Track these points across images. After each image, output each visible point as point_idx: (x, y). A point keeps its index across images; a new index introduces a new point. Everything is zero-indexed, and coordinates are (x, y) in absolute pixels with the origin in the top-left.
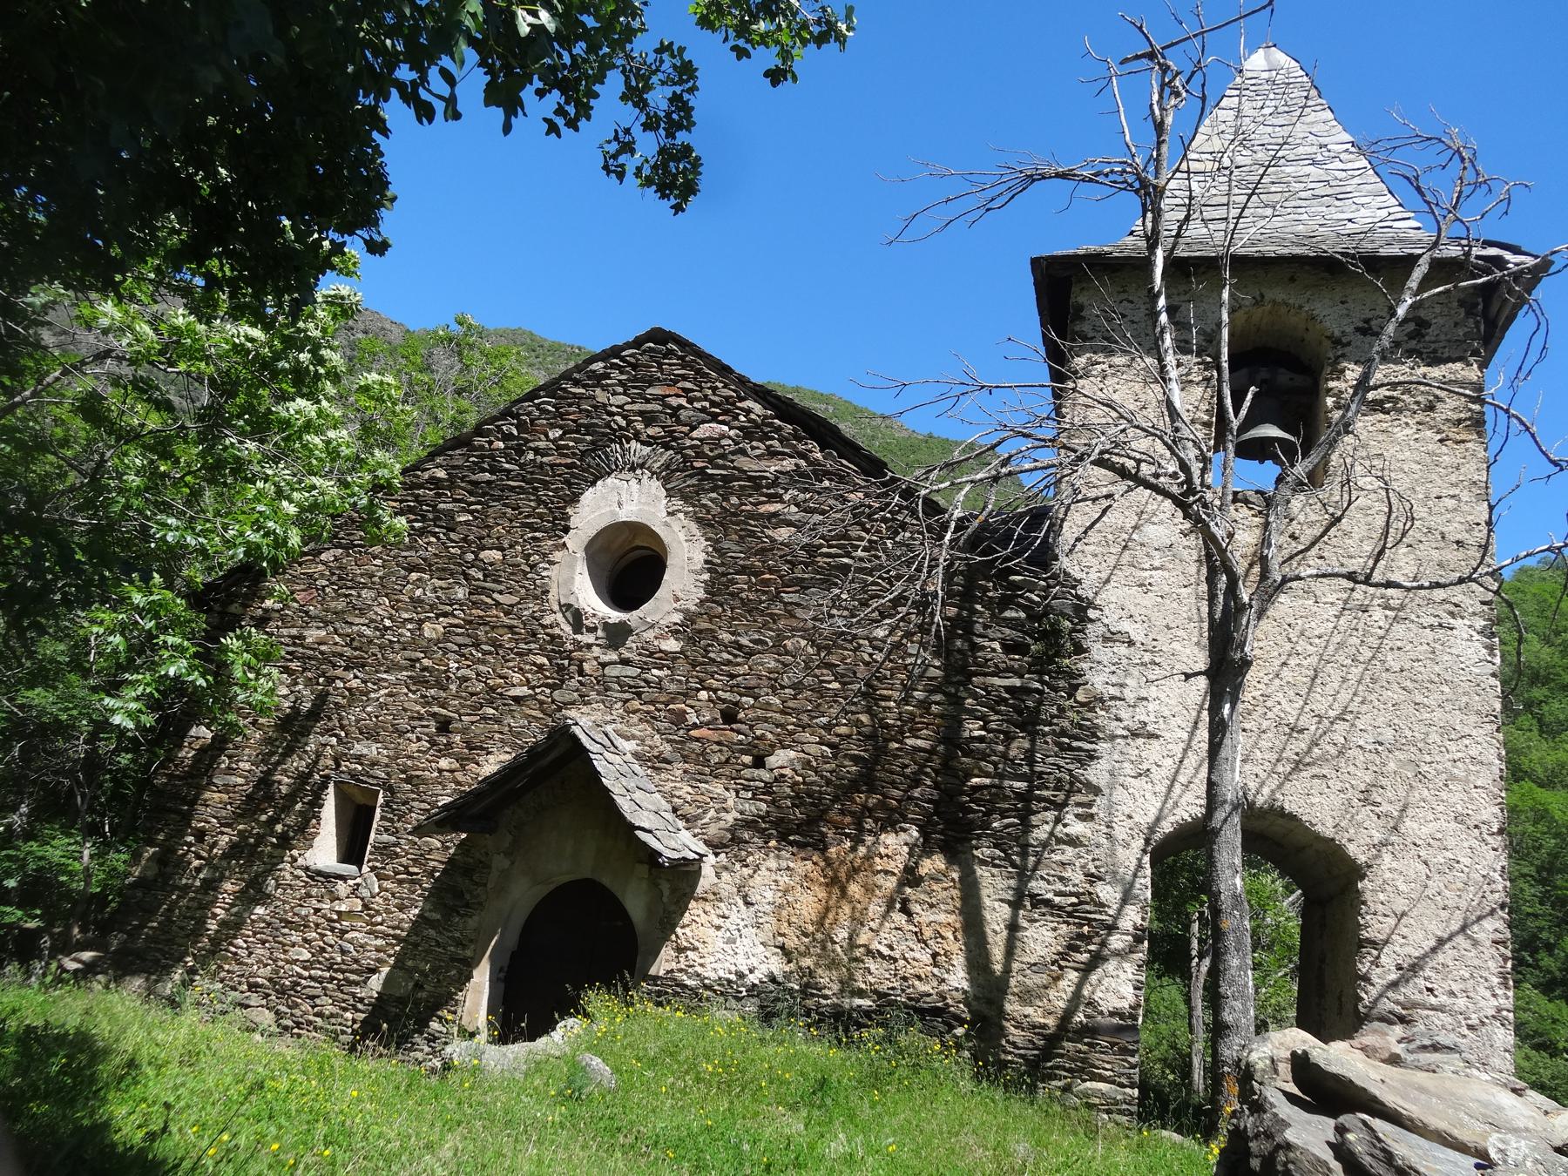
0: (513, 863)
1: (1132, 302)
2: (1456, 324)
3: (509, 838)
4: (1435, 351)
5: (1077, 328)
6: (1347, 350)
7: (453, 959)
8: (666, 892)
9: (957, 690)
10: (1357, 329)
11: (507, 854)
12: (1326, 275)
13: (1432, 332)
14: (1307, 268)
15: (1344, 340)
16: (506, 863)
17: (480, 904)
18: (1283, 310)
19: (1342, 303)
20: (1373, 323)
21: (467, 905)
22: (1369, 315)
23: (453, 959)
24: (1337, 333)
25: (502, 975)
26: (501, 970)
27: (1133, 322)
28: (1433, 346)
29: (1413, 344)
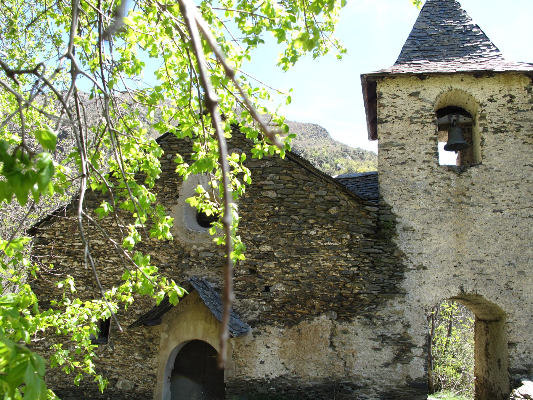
0: (169, 335)
1: (401, 91)
2: (525, 97)
3: (166, 326)
4: (518, 108)
5: (381, 102)
6: (485, 108)
7: (149, 375)
8: (234, 344)
9: (347, 255)
10: (488, 100)
11: (167, 332)
12: (474, 78)
13: (516, 101)
14: (467, 75)
15: (484, 104)
16: (167, 336)
17: (158, 353)
18: (460, 92)
19: (482, 89)
20: (494, 97)
21: (152, 353)
22: (492, 94)
23: (149, 375)
24: (481, 102)
25: (169, 380)
26: (169, 378)
27: (403, 99)
28: (517, 106)
29: (510, 105)
